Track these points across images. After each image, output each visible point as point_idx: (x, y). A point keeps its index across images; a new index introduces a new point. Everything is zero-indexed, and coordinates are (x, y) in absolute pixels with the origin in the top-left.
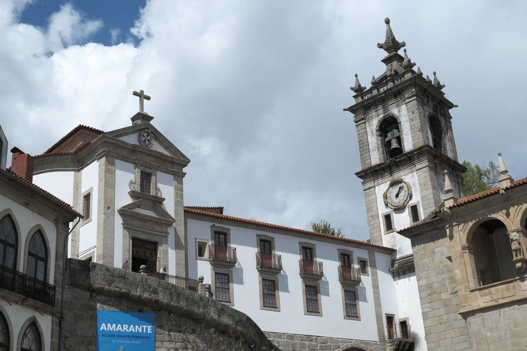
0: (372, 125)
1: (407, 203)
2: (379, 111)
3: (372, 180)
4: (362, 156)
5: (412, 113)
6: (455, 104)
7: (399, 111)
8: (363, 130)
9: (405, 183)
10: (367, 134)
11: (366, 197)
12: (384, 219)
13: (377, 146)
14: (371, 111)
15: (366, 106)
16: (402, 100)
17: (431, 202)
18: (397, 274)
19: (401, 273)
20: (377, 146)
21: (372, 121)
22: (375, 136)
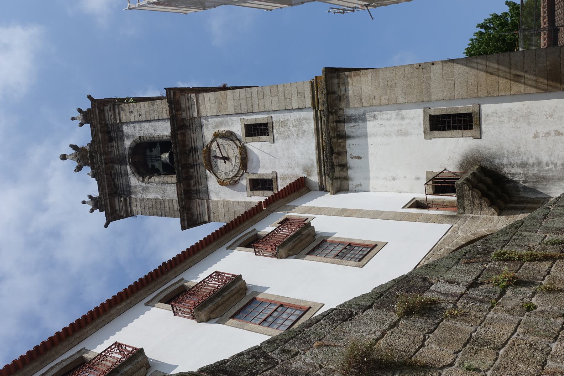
0: (136, 187)
1: (240, 142)
2: (123, 172)
3: (199, 201)
4: (167, 214)
5: (133, 115)
7: (128, 137)
8: (137, 203)
10: (143, 199)
11: (218, 220)
13: (161, 184)
14: (120, 184)
17: (245, 94)
18: (344, 182)
19: (343, 174)
20: (161, 184)
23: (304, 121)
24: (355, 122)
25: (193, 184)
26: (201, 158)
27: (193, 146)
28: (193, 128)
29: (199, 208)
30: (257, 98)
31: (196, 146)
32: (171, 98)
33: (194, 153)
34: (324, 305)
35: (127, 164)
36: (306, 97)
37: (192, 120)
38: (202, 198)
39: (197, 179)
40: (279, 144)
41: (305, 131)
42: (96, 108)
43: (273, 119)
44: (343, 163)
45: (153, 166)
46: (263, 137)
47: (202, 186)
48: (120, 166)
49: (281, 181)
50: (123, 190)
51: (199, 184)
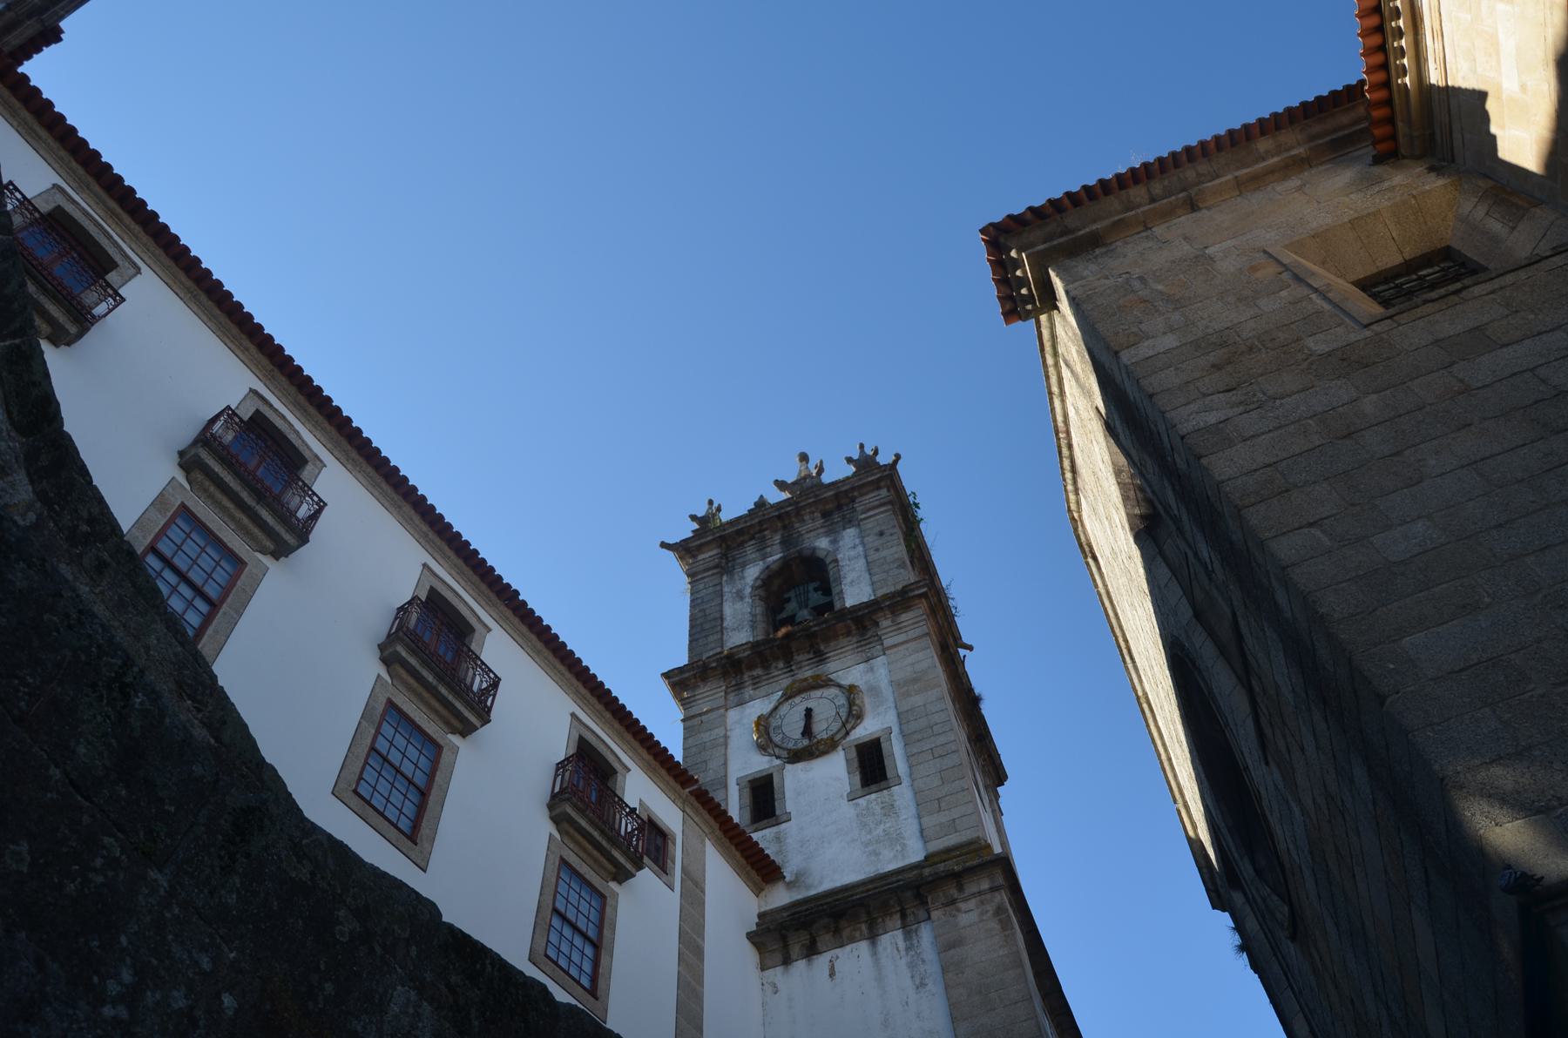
0: (743, 578)
2: (769, 550)
6: (966, 639)
7: (834, 542)
9: (839, 686)
10: (722, 596)
12: (747, 791)
15: (729, 543)
16: (846, 520)
17: (938, 721)
19: (795, 950)
21: (742, 571)
22: (748, 600)
23: (899, 848)
24: (908, 949)
25: (754, 673)
26: (807, 673)
27: (828, 655)
28: (861, 646)
29: (708, 696)
30: (933, 745)
31: (828, 660)
32: (912, 590)
33: (814, 660)
34: (425, 871)
35: (783, 552)
36: (947, 837)
37: (878, 641)
38: (728, 697)
39: (764, 678)
40: (848, 810)
41: (877, 854)
42: (879, 475)
43: (897, 787)
44: (819, 944)
45: (788, 600)
46: (857, 778)
47: (751, 692)
48: (780, 543)
49: (773, 835)
50: (734, 560)
51: (754, 684)
